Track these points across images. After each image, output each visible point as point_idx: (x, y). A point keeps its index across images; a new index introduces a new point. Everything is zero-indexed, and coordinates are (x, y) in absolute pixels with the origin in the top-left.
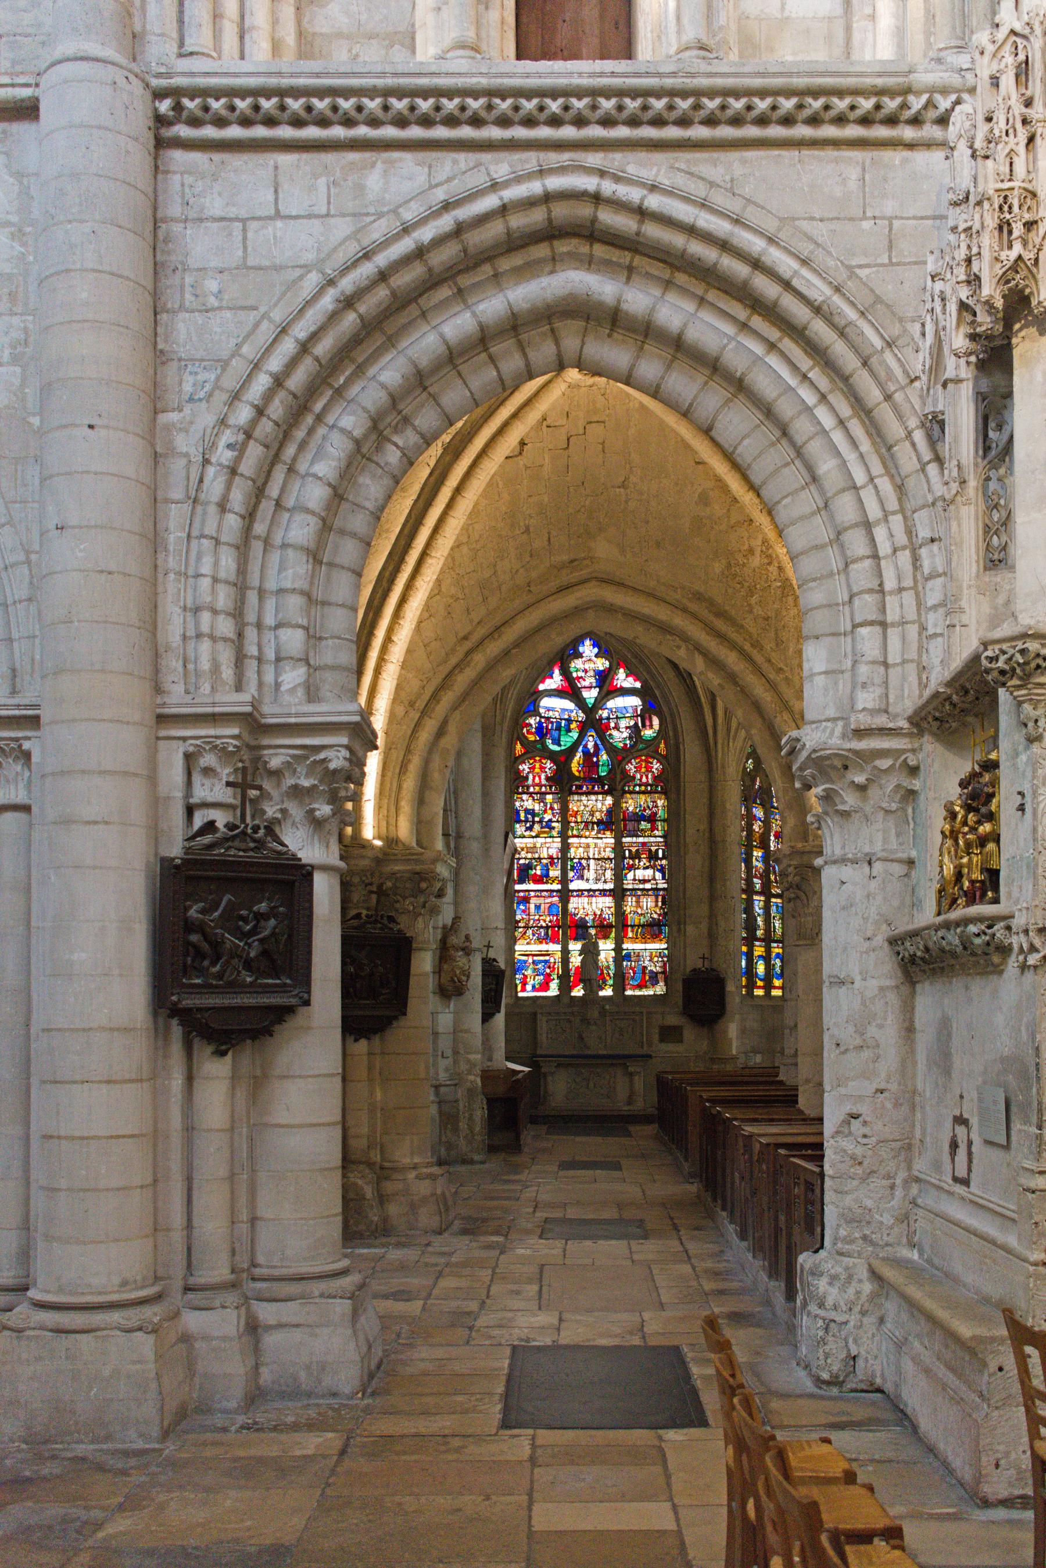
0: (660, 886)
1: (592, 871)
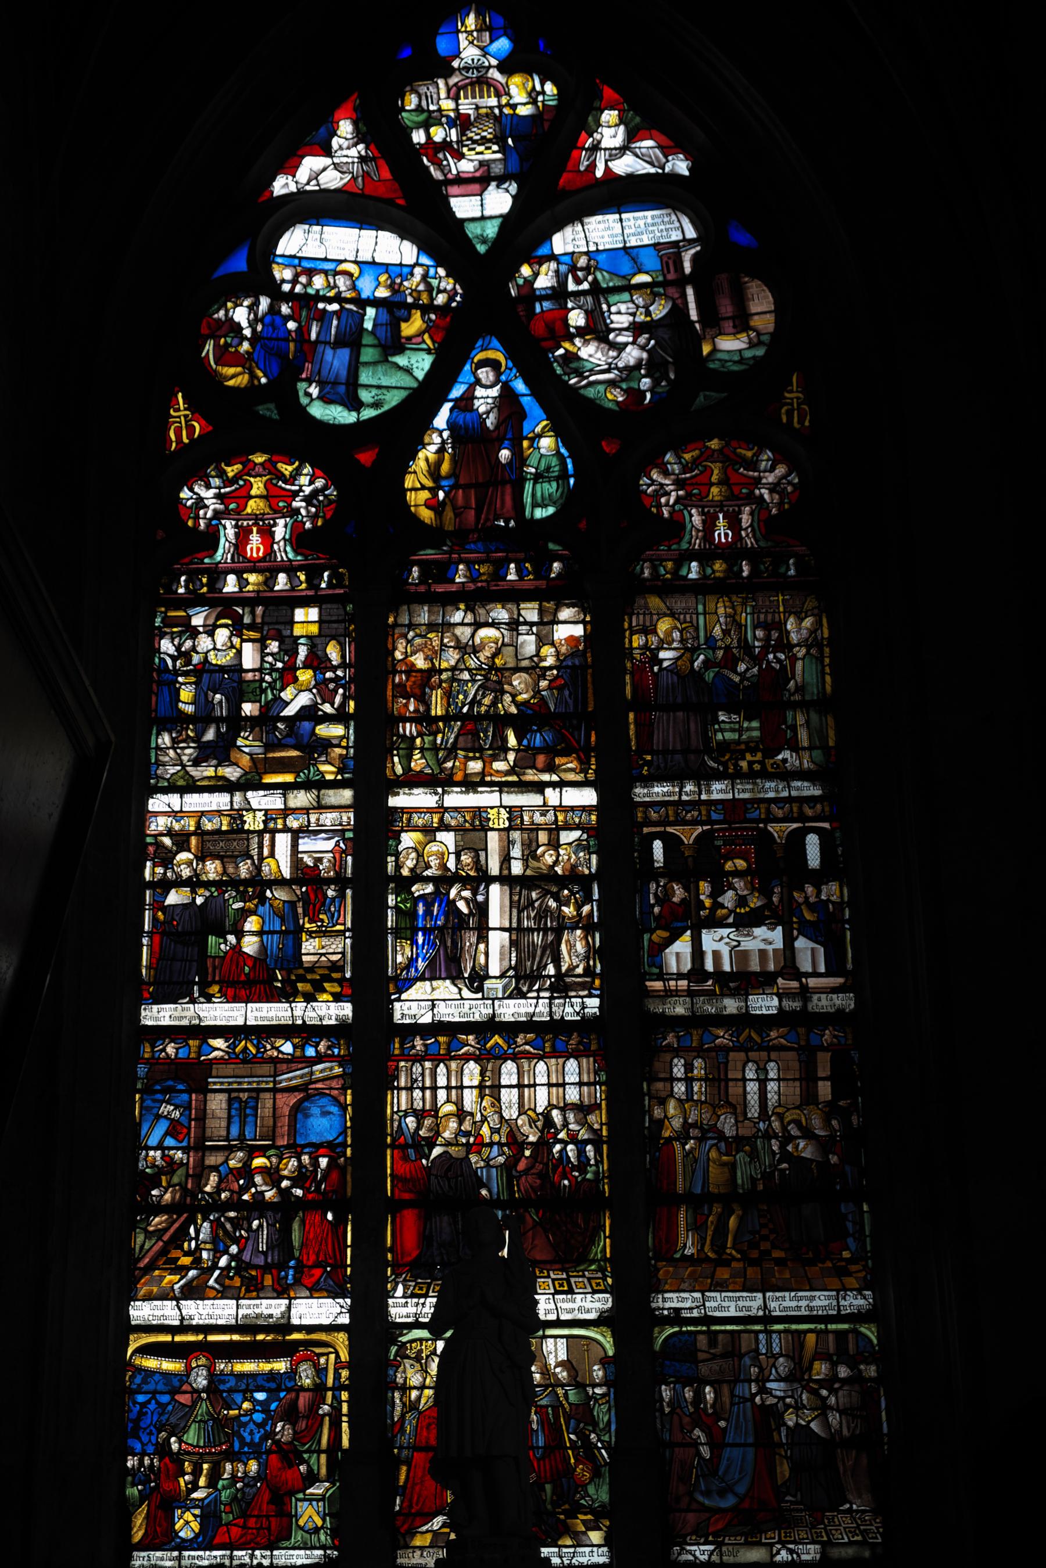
0: (822, 1003)
1: (498, 940)
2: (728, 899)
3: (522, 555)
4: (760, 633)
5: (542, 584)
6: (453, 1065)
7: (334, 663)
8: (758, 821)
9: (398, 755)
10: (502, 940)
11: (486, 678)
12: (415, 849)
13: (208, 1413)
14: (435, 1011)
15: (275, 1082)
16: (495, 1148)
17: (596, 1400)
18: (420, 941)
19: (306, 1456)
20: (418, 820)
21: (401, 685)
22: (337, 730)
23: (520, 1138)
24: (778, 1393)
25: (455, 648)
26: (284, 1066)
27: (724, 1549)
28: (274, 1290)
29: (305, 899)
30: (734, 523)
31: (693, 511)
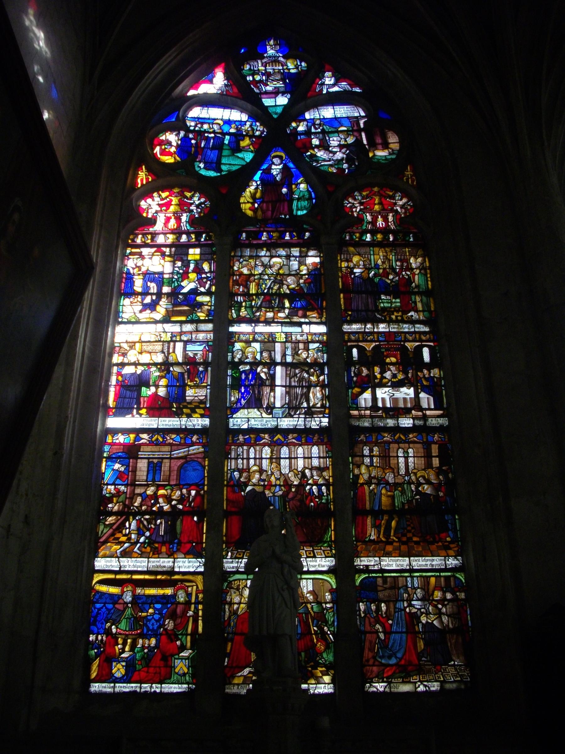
0: (433, 422)
1: (279, 391)
2: (388, 375)
3: (292, 229)
4: (398, 263)
5: (301, 241)
6: (258, 448)
7: (206, 271)
8: (401, 341)
9: (234, 309)
10: (282, 391)
11: (275, 278)
12: (241, 350)
13: (132, 614)
14: (249, 423)
15: (171, 454)
16: (278, 487)
17: (327, 610)
18: (243, 391)
19: (180, 637)
20: (243, 337)
21: (237, 280)
22: (205, 299)
23: (290, 483)
24: (418, 607)
25: (261, 266)
26: (176, 447)
27: (392, 685)
28: (167, 554)
29: (188, 371)
30: (386, 219)
31: (367, 214)
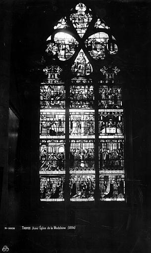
1: (82, 129)
2: (109, 124)
30: (111, 76)
